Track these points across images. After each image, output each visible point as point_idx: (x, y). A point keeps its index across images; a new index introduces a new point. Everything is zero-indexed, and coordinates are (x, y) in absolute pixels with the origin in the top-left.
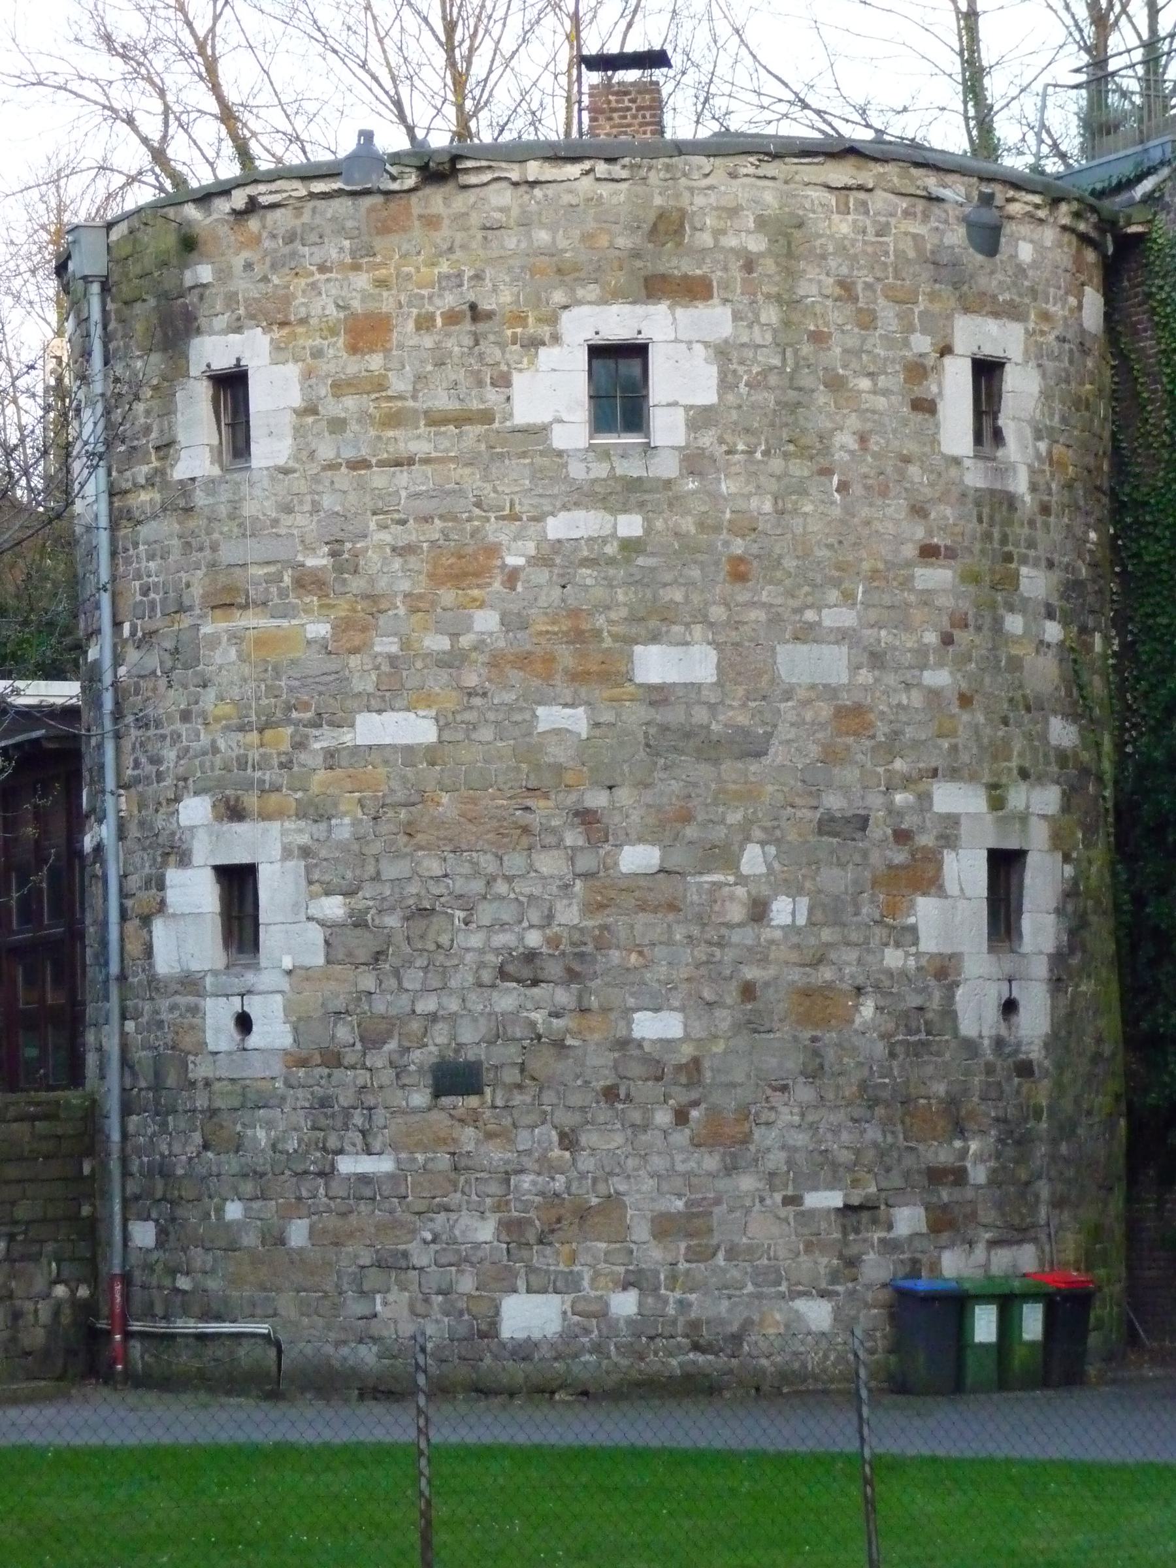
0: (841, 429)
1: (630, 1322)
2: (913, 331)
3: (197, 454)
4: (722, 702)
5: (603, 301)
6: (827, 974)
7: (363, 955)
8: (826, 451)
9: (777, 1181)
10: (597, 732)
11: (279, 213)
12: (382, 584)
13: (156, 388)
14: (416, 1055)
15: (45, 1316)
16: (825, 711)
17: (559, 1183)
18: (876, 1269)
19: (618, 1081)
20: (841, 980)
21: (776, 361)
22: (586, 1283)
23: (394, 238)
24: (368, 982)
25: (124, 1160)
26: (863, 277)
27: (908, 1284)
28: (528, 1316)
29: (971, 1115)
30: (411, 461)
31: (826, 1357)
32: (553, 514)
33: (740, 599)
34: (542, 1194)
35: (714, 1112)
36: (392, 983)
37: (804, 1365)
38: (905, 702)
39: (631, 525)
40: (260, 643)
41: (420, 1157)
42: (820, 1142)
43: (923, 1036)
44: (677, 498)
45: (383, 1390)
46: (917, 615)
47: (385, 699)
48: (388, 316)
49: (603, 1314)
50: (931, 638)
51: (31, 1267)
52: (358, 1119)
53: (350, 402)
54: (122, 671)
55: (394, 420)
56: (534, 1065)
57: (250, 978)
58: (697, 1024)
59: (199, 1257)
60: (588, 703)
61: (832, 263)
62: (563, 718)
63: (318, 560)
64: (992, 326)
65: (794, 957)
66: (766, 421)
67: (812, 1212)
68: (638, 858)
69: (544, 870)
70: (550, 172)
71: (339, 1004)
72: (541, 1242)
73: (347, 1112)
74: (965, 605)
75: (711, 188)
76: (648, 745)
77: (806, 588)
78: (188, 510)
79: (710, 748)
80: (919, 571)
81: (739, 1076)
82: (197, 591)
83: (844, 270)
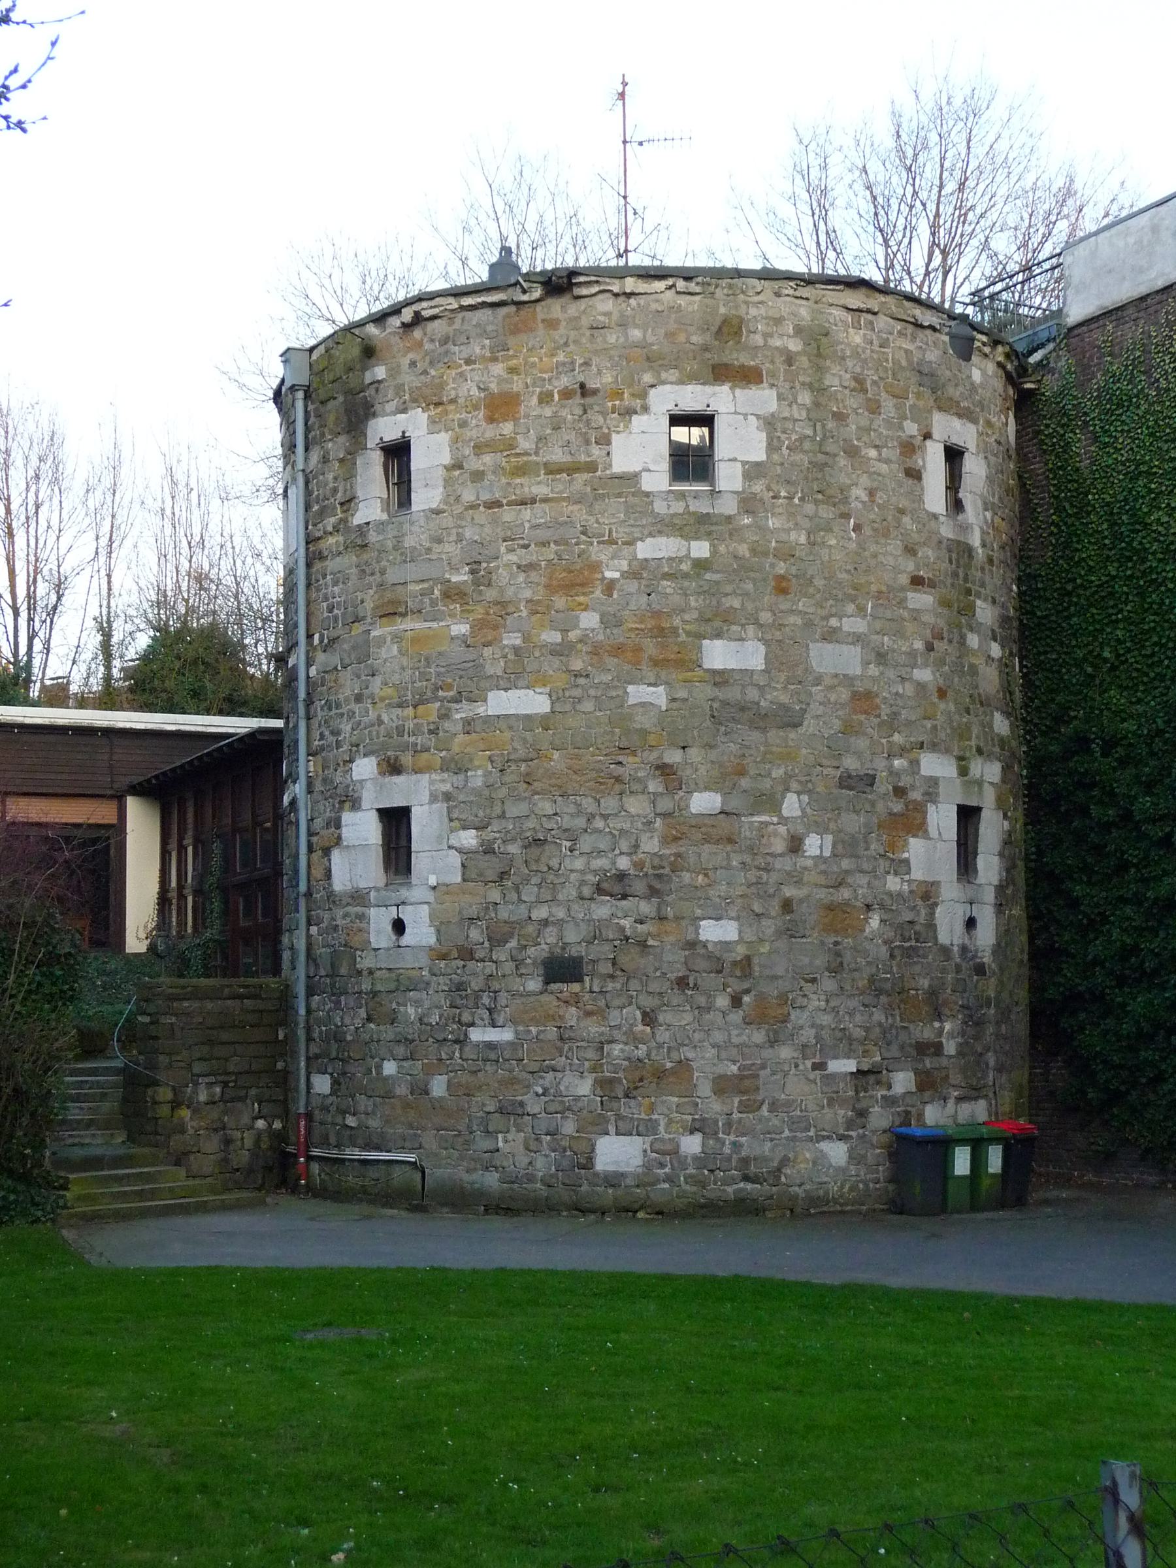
0: (857, 485)
1: (696, 1158)
2: (906, 419)
3: (371, 507)
4: (769, 685)
5: (681, 382)
6: (845, 894)
7: (491, 875)
8: (846, 500)
9: (808, 1051)
10: (675, 705)
11: (437, 322)
12: (510, 592)
13: (341, 461)
14: (531, 951)
15: (249, 1143)
16: (844, 695)
17: (641, 1052)
18: (880, 1119)
19: (688, 973)
20: (856, 898)
21: (809, 432)
22: (661, 1129)
23: (523, 337)
24: (495, 895)
25: (308, 1029)
26: (871, 376)
27: (903, 1130)
28: (617, 1153)
29: (946, 1003)
30: (533, 501)
31: (842, 1187)
32: (641, 540)
33: (783, 607)
34: (628, 1059)
35: (761, 998)
36: (514, 896)
37: (827, 1193)
38: (901, 691)
39: (701, 549)
40: (416, 640)
41: (534, 1030)
42: (840, 1022)
43: (913, 943)
44: (736, 530)
45: (504, 1207)
46: (910, 627)
47: (511, 680)
48: (518, 394)
49: (675, 1152)
50: (919, 645)
51: (239, 1105)
52: (486, 1000)
53: (488, 459)
54: (313, 672)
55: (521, 470)
56: (624, 960)
57: (404, 893)
58: (749, 930)
59: (363, 1102)
60: (666, 683)
61: (850, 363)
62: (647, 695)
63: (461, 577)
64: (957, 423)
65: (822, 880)
66: (802, 475)
67: (833, 1076)
68: (704, 802)
69: (632, 810)
70: (642, 286)
71: (473, 912)
72: (627, 1096)
73: (477, 996)
74: (941, 623)
75: (761, 303)
76: (713, 717)
77: (831, 602)
78: (364, 546)
79: (760, 719)
80: (910, 595)
82: (369, 605)
83: (858, 370)
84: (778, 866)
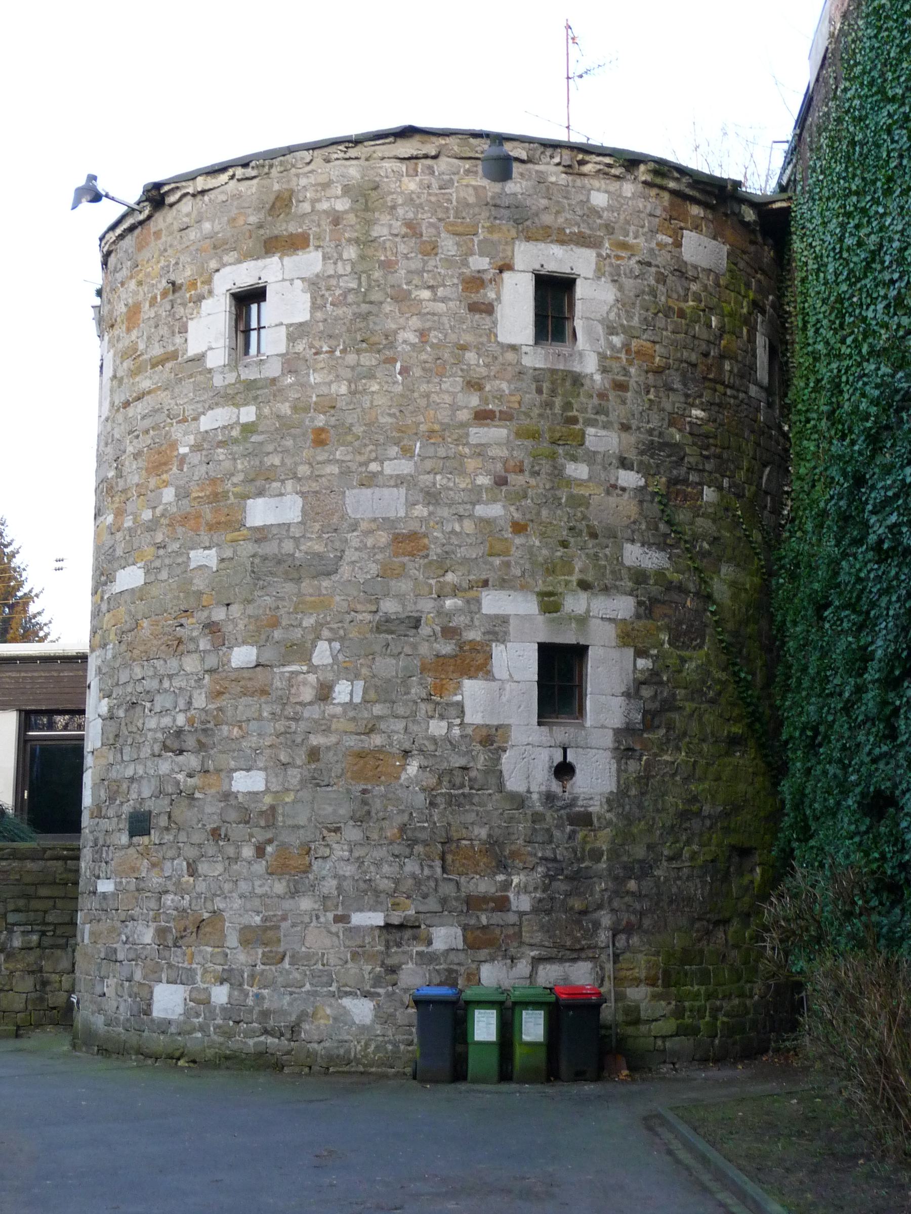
0: (404, 329)
1: (223, 1009)
2: (472, 254)
4: (303, 536)
5: (239, 261)
6: (377, 740)
8: (391, 345)
9: (329, 903)
10: (223, 565)
16: (383, 538)
19: (221, 824)
20: (391, 745)
21: (353, 285)
22: (198, 978)
26: (427, 218)
30: (144, 395)
31: (367, 1045)
32: (204, 414)
33: (319, 458)
34: (176, 909)
37: (348, 1051)
38: (458, 529)
39: (248, 414)
42: (365, 872)
43: (466, 790)
44: (279, 391)
46: (471, 464)
49: (207, 1002)
50: (484, 480)
51: (59, 952)
58: (274, 780)
60: (218, 545)
61: (400, 211)
62: (204, 558)
65: (351, 727)
66: (344, 329)
67: (358, 928)
68: (243, 656)
70: (211, 182)
72: (175, 946)
75: (311, 172)
76: (253, 572)
77: (371, 447)
80: (473, 430)
81: (302, 820)
83: (410, 215)
84: (306, 714)
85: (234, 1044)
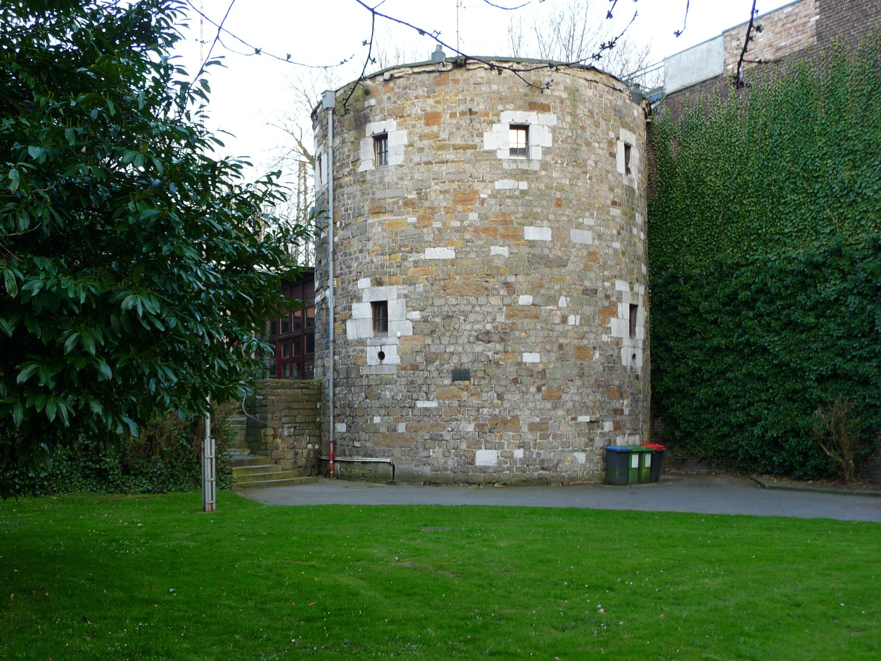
1: (520, 460)
3: (367, 163)
5: (515, 110)
6: (585, 342)
7: (427, 332)
8: (585, 166)
11: (401, 80)
12: (436, 203)
13: (352, 142)
14: (446, 366)
15: (305, 455)
16: (585, 253)
17: (497, 411)
18: (599, 442)
21: (570, 134)
22: (506, 446)
23: (442, 87)
24: (429, 341)
25: (334, 402)
26: (596, 111)
27: (609, 447)
28: (485, 458)
29: (625, 391)
30: (447, 162)
35: (550, 388)
36: (438, 341)
39: (523, 185)
40: (390, 225)
41: (447, 402)
45: (432, 482)
46: (611, 223)
47: (437, 242)
48: (440, 113)
49: (511, 457)
50: (615, 232)
52: (424, 388)
53: (426, 142)
54: (336, 239)
55: (441, 148)
56: (489, 371)
57: (384, 340)
59: (363, 435)
61: (587, 104)
62: (500, 251)
63: (413, 196)
64: (629, 133)
65: (575, 336)
67: (580, 423)
68: (525, 300)
69: (493, 303)
71: (418, 348)
73: (420, 386)
74: (623, 222)
78: (364, 182)
79: (549, 263)
81: (558, 376)
82: (366, 209)
84: (557, 329)
85: (528, 475)
